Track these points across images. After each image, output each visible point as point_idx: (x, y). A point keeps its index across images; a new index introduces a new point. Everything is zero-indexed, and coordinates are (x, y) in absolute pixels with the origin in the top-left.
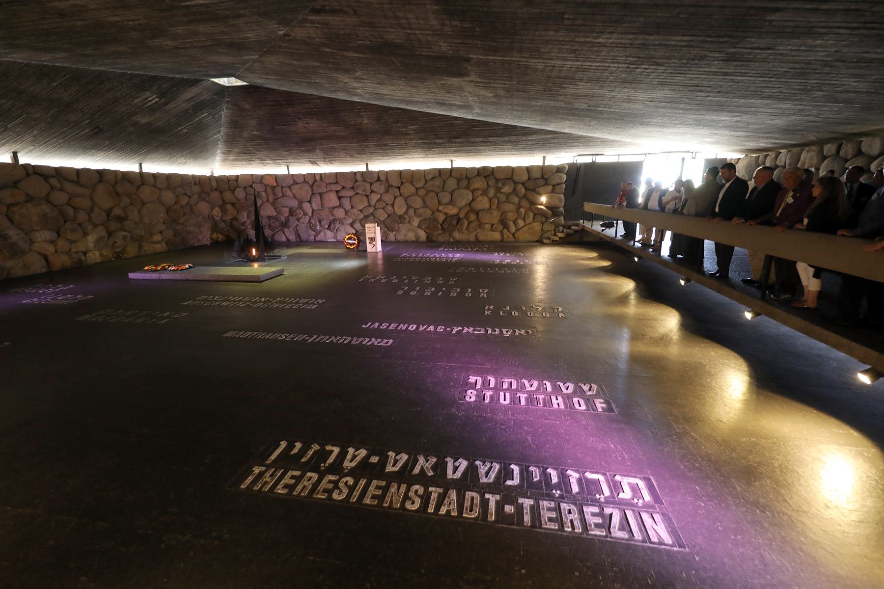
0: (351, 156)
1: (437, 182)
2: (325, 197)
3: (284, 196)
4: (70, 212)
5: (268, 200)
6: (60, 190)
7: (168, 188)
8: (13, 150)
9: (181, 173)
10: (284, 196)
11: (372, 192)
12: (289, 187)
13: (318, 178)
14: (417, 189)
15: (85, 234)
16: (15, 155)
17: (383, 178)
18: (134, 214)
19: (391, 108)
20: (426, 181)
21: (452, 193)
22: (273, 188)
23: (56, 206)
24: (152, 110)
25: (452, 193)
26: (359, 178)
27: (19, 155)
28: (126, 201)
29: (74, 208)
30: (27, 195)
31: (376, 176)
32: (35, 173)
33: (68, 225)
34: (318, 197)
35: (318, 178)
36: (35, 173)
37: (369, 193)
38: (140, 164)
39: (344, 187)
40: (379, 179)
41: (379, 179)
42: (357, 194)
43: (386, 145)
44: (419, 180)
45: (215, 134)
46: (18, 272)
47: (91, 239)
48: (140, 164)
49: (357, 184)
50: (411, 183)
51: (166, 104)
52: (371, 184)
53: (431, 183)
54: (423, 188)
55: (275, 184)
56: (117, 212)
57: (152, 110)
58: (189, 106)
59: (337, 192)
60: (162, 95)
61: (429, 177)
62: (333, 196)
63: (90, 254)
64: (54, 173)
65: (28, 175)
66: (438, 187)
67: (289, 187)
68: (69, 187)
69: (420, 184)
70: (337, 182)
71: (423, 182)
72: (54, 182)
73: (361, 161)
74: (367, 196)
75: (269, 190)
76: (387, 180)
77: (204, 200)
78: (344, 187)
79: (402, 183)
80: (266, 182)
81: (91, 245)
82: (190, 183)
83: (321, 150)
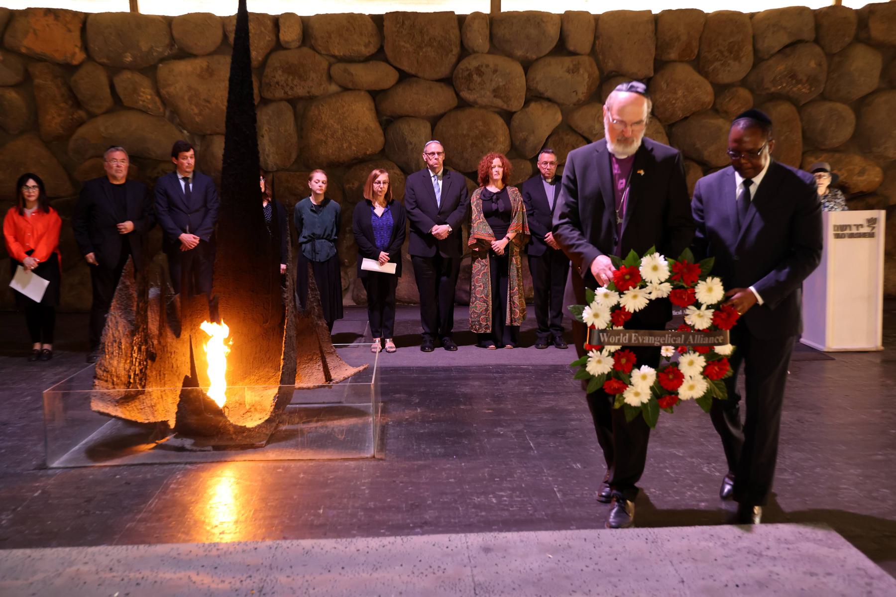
1: (809, 62)
2: (325, 114)
3: (118, 104)
5: (34, 125)
10: (118, 104)
11: (533, 96)
12: (149, 69)
13: (290, 35)
14: (720, 89)
17: (580, 41)
20: (759, 59)
21: (860, 105)
22: (69, 69)
25: (860, 105)
26: (479, 39)
31: (553, 32)
34: (289, 115)
35: (290, 35)
37: (516, 105)
39: (404, 77)
40: (561, 48)
41: (561, 48)
42: (463, 104)
44: (734, 52)
49: (471, 63)
50: (699, 65)
52: (527, 66)
53: (780, 67)
54: (744, 83)
55: (80, 56)
59: (377, 95)
61: (774, 42)
62: (361, 112)
66: (812, 80)
67: (149, 69)
69: (734, 71)
70: (380, 55)
71: (748, 60)
74: (508, 116)
75: (44, 81)
76: (593, 53)
78: (404, 77)
79: (660, 64)
80: (28, 44)
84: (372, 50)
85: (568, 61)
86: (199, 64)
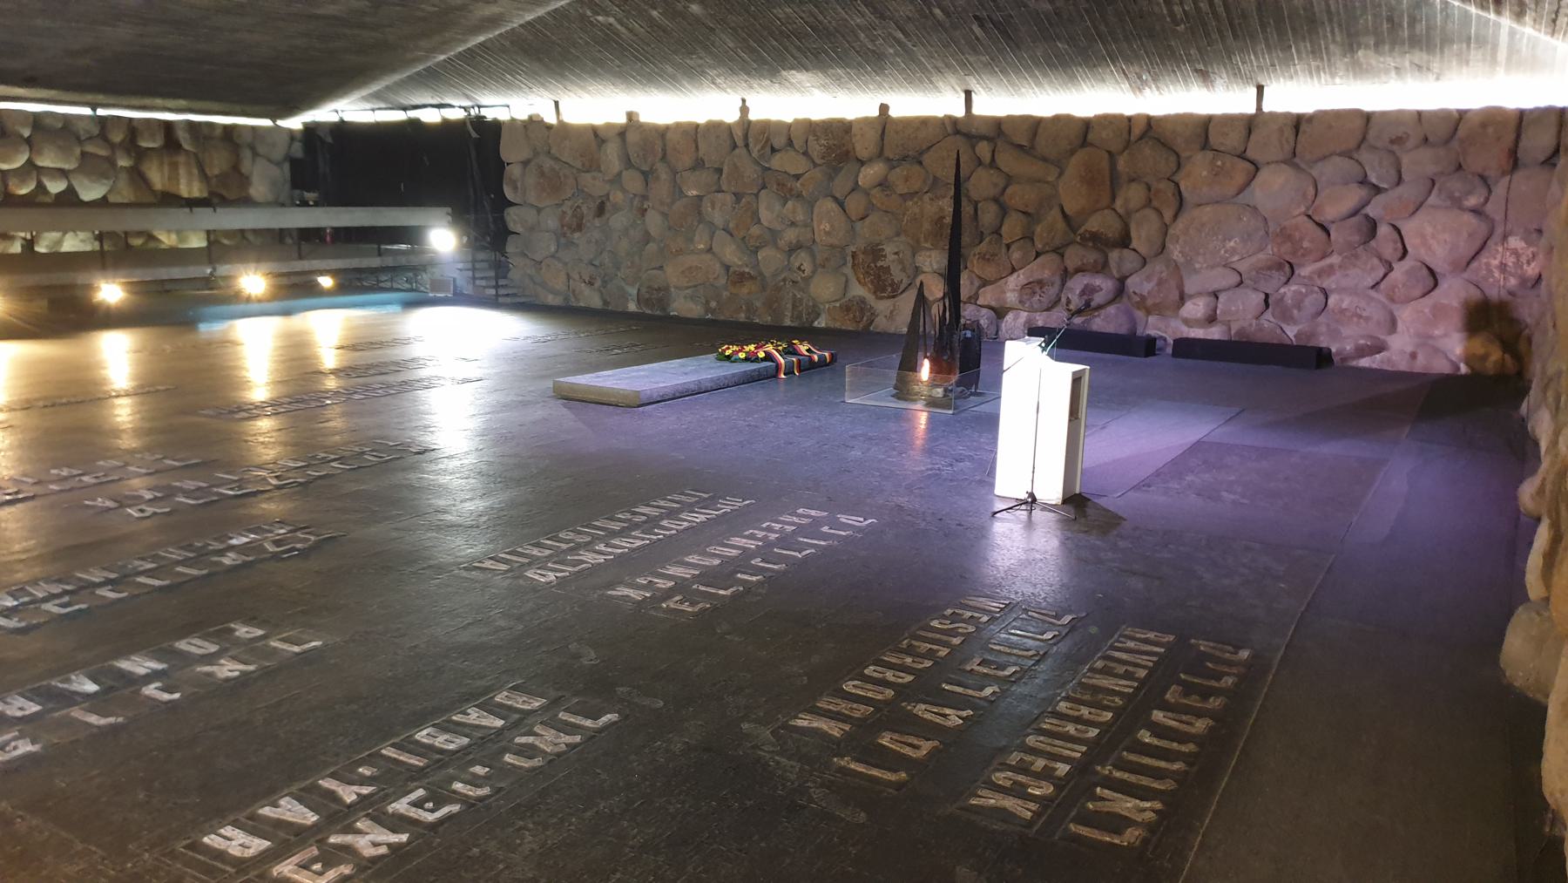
4: (988, 215)
7: (1291, 159)
9: (1367, 107)
15: (1014, 270)
18: (1141, 238)
28: (1132, 195)
32: (957, 132)
33: (983, 247)
36: (957, 132)
46: (881, 324)
47: (1014, 282)
56: (1093, 224)
63: (1009, 317)
64: (983, 131)
68: (1007, 160)
77: (1456, 203)
81: (1011, 297)
82: (1398, 141)
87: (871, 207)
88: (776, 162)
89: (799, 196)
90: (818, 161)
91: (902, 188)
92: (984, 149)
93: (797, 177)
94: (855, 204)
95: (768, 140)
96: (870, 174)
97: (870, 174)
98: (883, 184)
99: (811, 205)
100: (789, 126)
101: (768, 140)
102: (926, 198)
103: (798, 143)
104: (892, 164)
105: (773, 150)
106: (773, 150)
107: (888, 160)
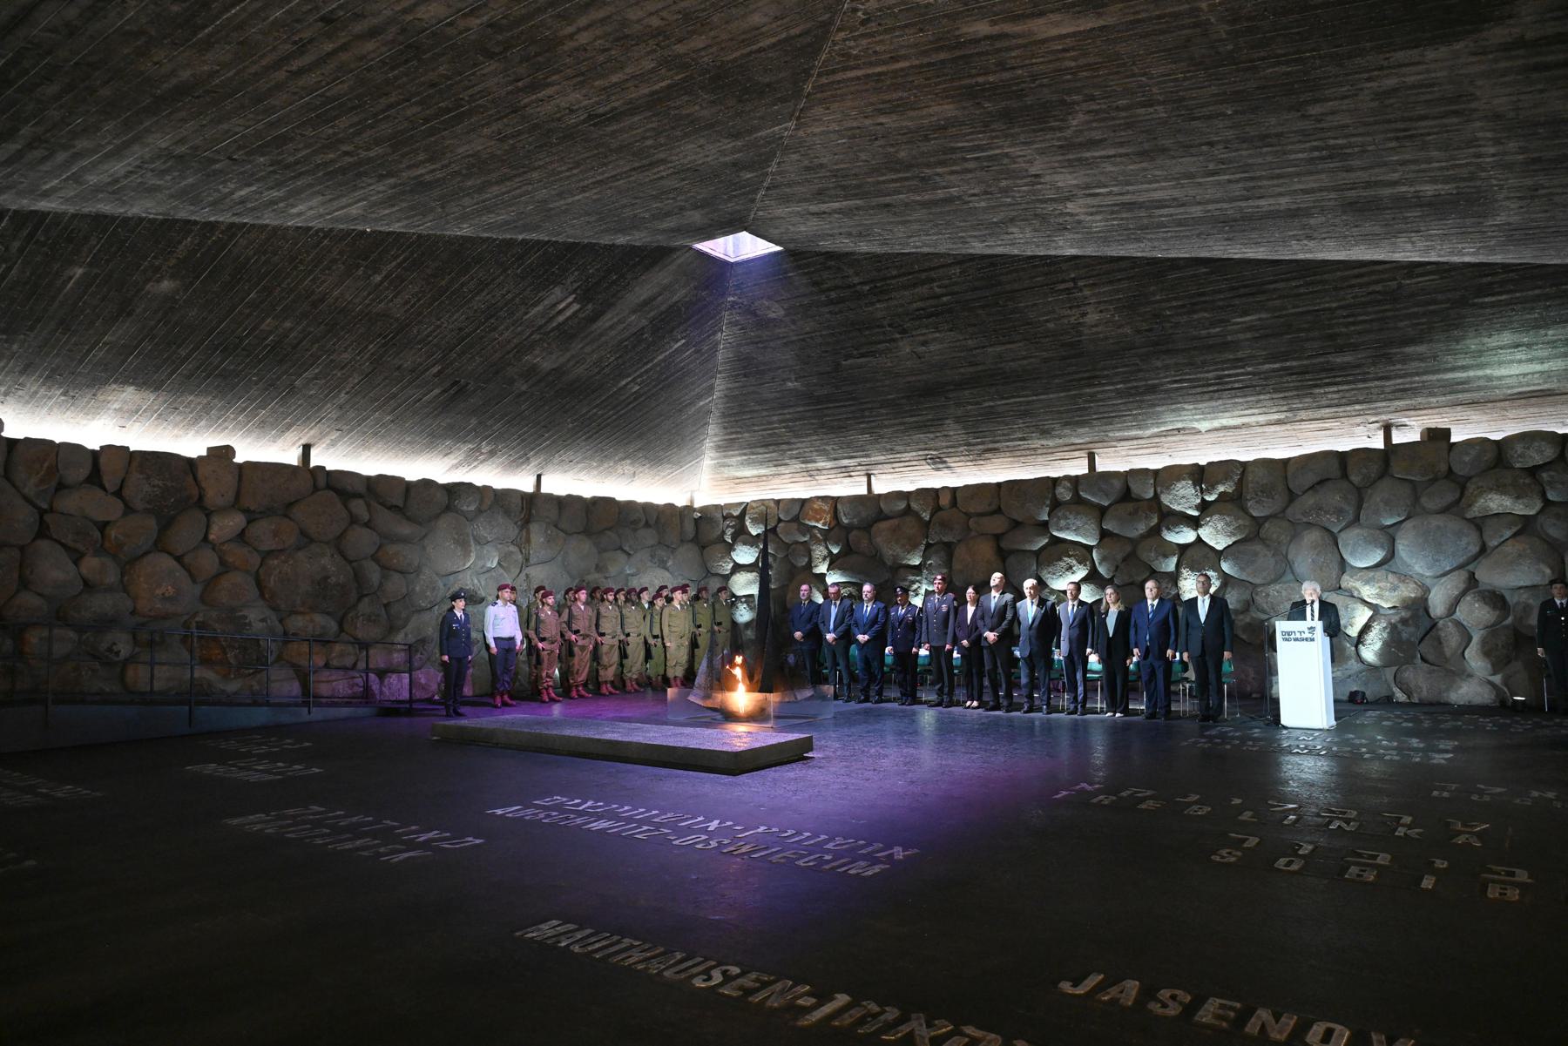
0: (1045, 433)
6: (367, 525)
8: (303, 441)
13: (945, 501)
16: (307, 449)
19: (1174, 264)
23: (350, 562)
24: (566, 334)
27: (313, 452)
29: (383, 567)
30: (303, 533)
31: (1117, 484)
35: (945, 501)
36: (329, 487)
38: (539, 477)
40: (1126, 496)
43: (1153, 389)
45: (700, 397)
48: (539, 477)
51: (593, 319)
57: (566, 334)
58: (644, 322)
60: (585, 296)
64: (362, 489)
65: (316, 489)
68: (385, 519)
70: (998, 511)
72: (358, 507)
73: (1075, 447)
83: (958, 420)
84: (994, 507)
85: (1130, 506)
86: (896, 521)
87: (225, 567)
88: (70, 503)
89: (101, 550)
90: (138, 504)
91: (268, 544)
92: (358, 507)
93: (103, 526)
94: (207, 562)
95: (53, 470)
96: (227, 525)
97: (227, 525)
98: (241, 537)
99: (128, 565)
100: (95, 455)
101: (53, 470)
102: (300, 555)
103: (110, 482)
104: (252, 517)
105: (61, 486)
106: (61, 486)
107: (246, 511)
